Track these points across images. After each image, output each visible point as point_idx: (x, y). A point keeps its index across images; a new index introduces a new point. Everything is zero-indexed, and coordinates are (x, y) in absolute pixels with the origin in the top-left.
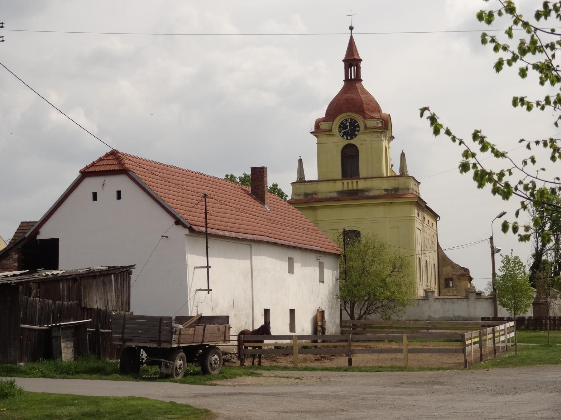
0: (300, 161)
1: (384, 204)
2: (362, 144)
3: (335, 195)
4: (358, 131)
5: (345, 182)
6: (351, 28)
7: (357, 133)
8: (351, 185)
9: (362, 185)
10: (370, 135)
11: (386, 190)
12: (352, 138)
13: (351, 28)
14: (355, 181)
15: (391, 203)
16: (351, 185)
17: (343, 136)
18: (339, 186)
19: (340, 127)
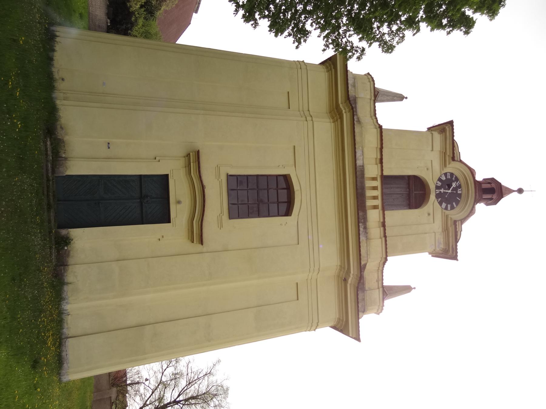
0: (400, 98)
1: (344, 268)
2: (429, 214)
3: (359, 163)
4: (446, 208)
5: (378, 183)
6: (520, 191)
7: (444, 205)
8: (373, 193)
9: (373, 216)
10: (440, 230)
11: (365, 265)
12: (438, 196)
13: (520, 191)
14: (378, 202)
15: (345, 280)
16: (373, 193)
17: (440, 180)
18: (372, 171)
19: (452, 174)
